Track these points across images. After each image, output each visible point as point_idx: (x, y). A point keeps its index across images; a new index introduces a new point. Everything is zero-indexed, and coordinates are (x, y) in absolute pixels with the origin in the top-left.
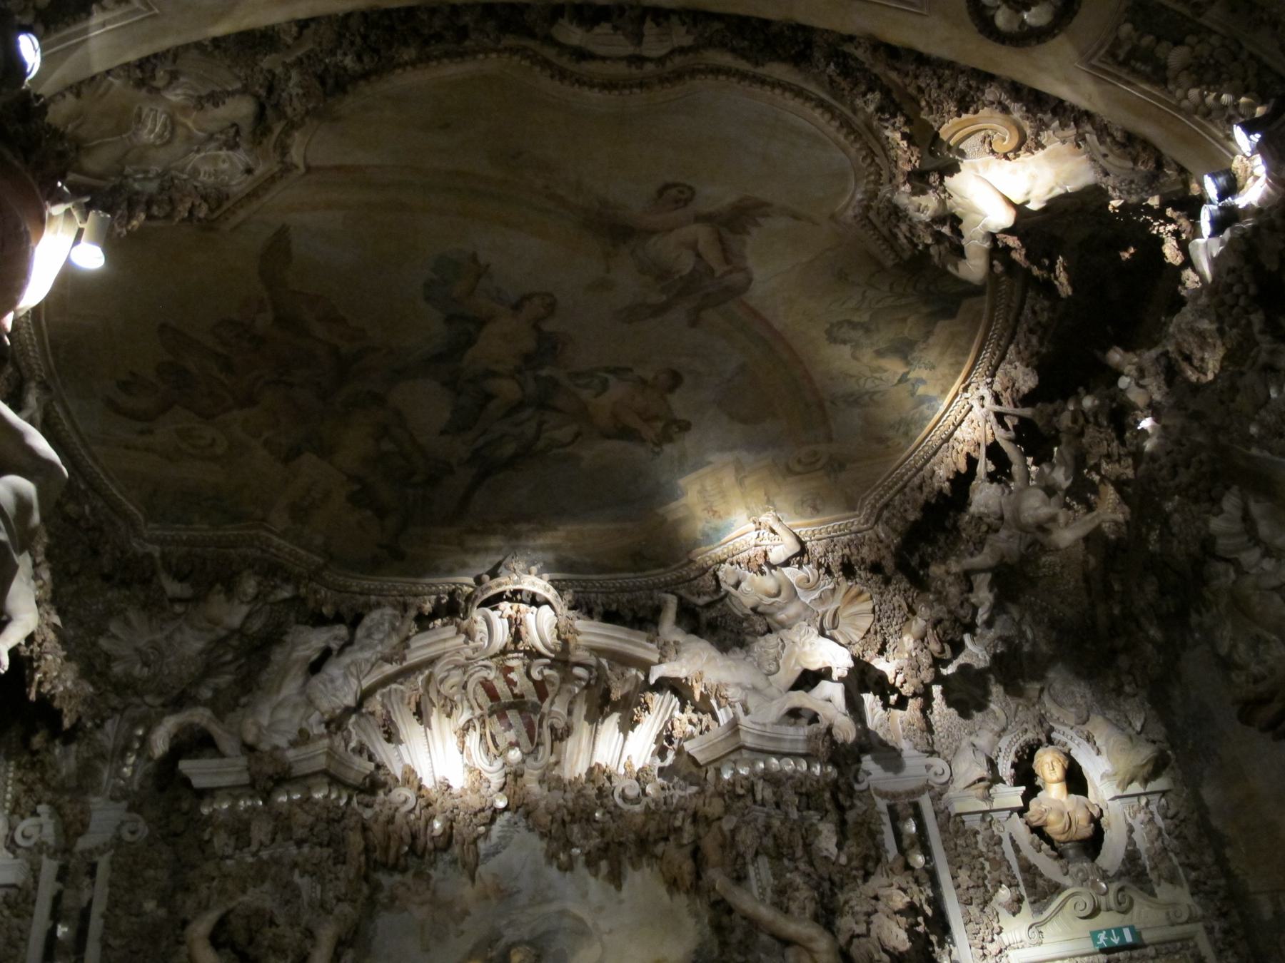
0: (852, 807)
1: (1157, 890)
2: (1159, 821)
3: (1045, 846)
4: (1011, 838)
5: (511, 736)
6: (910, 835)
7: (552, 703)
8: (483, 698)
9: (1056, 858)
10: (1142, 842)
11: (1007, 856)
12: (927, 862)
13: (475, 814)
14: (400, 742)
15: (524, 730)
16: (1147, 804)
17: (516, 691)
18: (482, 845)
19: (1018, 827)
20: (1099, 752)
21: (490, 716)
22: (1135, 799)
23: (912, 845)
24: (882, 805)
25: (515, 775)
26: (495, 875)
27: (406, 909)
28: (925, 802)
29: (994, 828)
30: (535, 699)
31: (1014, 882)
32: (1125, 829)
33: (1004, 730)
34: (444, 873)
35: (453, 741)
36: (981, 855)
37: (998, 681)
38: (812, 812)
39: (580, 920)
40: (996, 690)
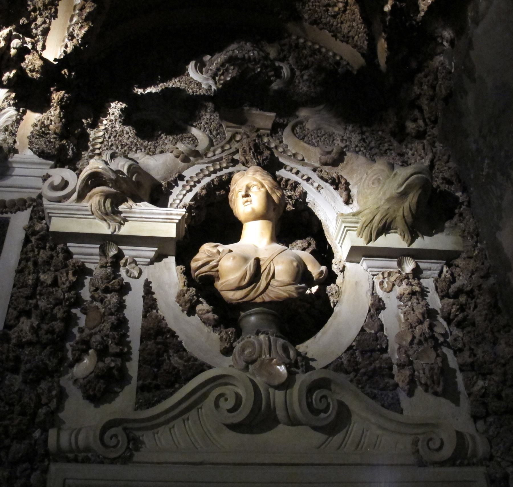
1: (405, 401)
2: (435, 301)
3: (203, 306)
4: (147, 285)
9: (216, 325)
10: (393, 318)
11: (127, 313)
16: (417, 272)
19: (168, 276)
20: (348, 201)
22: (394, 263)
29: (123, 272)
31: (114, 349)
32: (367, 302)
33: (197, 154)
36: (78, 302)
37: (216, 109)
40: (208, 116)
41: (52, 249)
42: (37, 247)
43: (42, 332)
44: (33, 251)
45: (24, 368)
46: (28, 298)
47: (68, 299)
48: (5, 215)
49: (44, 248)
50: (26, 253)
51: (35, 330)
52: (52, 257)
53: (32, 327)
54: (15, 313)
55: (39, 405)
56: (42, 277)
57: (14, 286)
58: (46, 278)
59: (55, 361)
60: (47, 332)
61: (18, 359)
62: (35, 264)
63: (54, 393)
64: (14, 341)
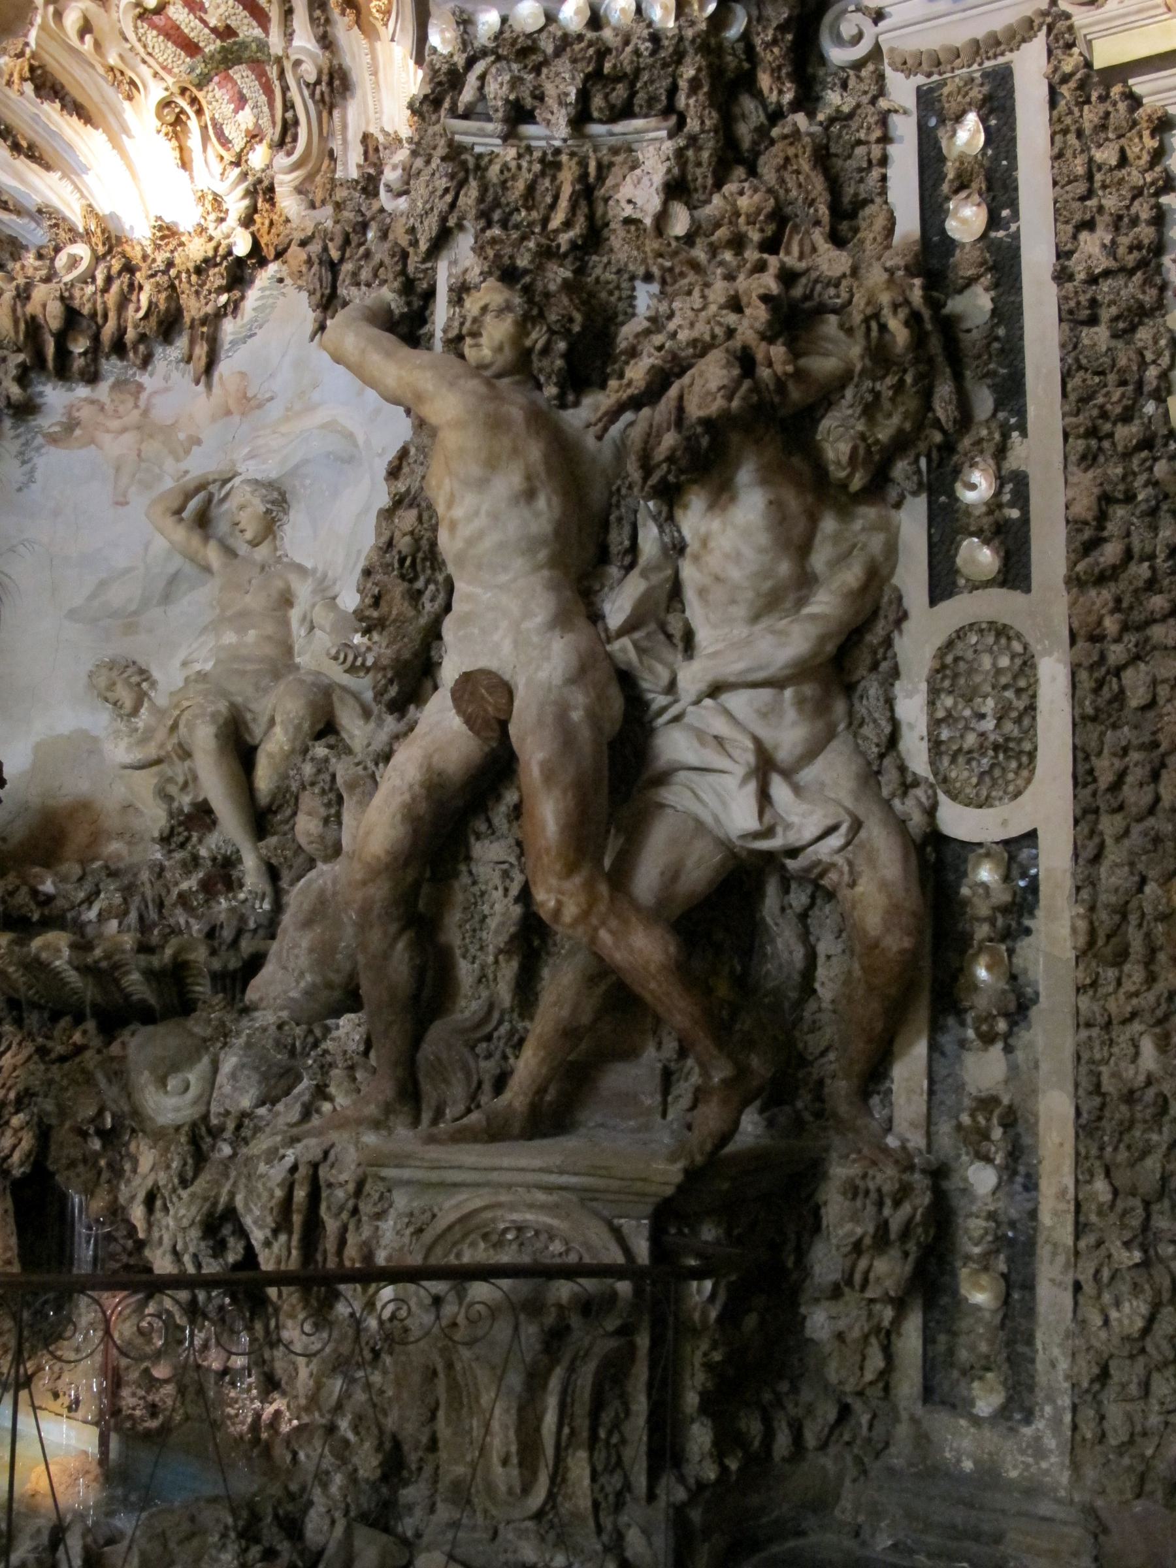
0: (807, 100)
5: (246, 118)
6: (961, 158)
7: (289, 35)
8: (167, 52)
12: (994, 221)
13: (199, 271)
14: (86, 169)
15: (263, 99)
17: (213, 22)
18: (229, 327)
21: (200, 87)
23: (962, 185)
24: (902, 91)
25: (262, 191)
26: (243, 375)
27: (93, 441)
28: (1030, 67)
30: (258, 32)
34: (166, 379)
35: (167, 150)
38: (638, 123)
39: (350, 437)
41: (1103, 99)
42: (1078, 104)
43: (1121, 250)
44: (1070, 112)
45: (1106, 314)
46: (1083, 199)
47: (1153, 183)
48: (1001, 60)
49: (1088, 101)
50: (1059, 120)
51: (1111, 249)
52: (1107, 114)
53: (1104, 246)
54: (1069, 229)
55: (1143, 364)
56: (1099, 155)
57: (1055, 183)
58: (1106, 155)
59: (1154, 292)
60: (1131, 249)
61: (1094, 303)
62: (1080, 134)
63: (1163, 342)
64: (1082, 276)
